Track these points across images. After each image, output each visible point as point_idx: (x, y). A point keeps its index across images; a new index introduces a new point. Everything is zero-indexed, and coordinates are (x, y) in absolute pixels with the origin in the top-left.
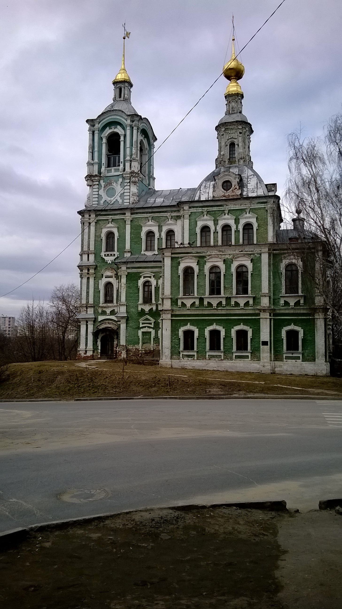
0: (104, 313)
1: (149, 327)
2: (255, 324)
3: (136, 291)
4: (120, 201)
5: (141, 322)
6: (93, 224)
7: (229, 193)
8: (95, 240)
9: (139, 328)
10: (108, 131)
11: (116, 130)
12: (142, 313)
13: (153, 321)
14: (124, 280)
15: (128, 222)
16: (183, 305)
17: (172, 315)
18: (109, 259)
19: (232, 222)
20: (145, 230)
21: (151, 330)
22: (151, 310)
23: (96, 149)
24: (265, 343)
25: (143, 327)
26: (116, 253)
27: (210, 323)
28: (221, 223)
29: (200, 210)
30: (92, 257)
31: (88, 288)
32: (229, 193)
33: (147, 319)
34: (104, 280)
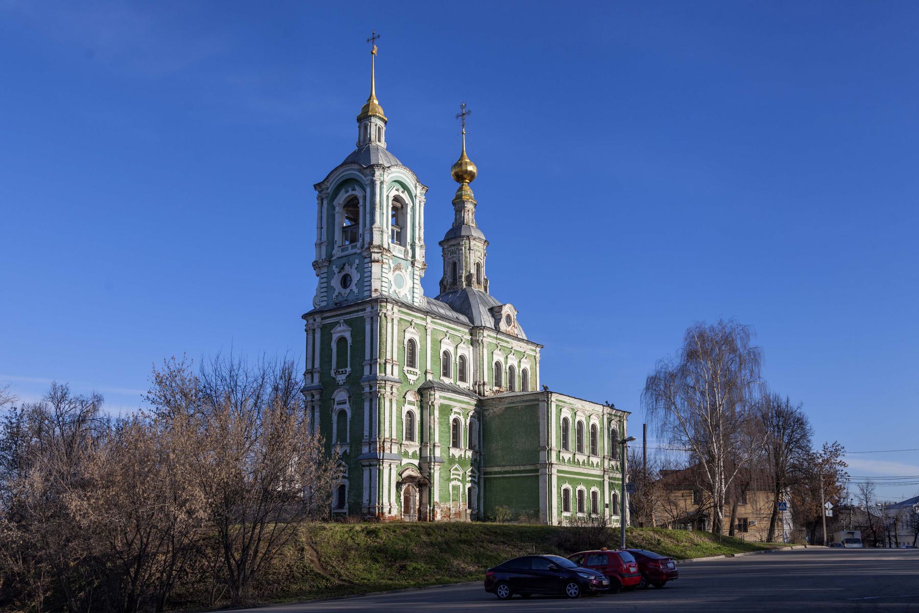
0: (406, 454)
1: (459, 480)
2: (601, 485)
3: (447, 430)
4: (410, 298)
5: (452, 472)
6: (395, 322)
7: (509, 329)
8: (398, 348)
9: (449, 480)
10: (394, 193)
11: (402, 195)
12: (452, 460)
13: (461, 473)
14: (437, 413)
15: (429, 331)
16: (564, 460)
17: (559, 471)
18: (411, 377)
19: (516, 364)
20: (444, 348)
21: (459, 483)
22: (460, 457)
23: (385, 212)
24: (607, 506)
25: (455, 479)
26: (419, 372)
27: (579, 482)
28: (510, 363)
29: (494, 341)
30: (396, 369)
31: (391, 416)
32: (509, 329)
33: (456, 469)
34: (407, 408)
